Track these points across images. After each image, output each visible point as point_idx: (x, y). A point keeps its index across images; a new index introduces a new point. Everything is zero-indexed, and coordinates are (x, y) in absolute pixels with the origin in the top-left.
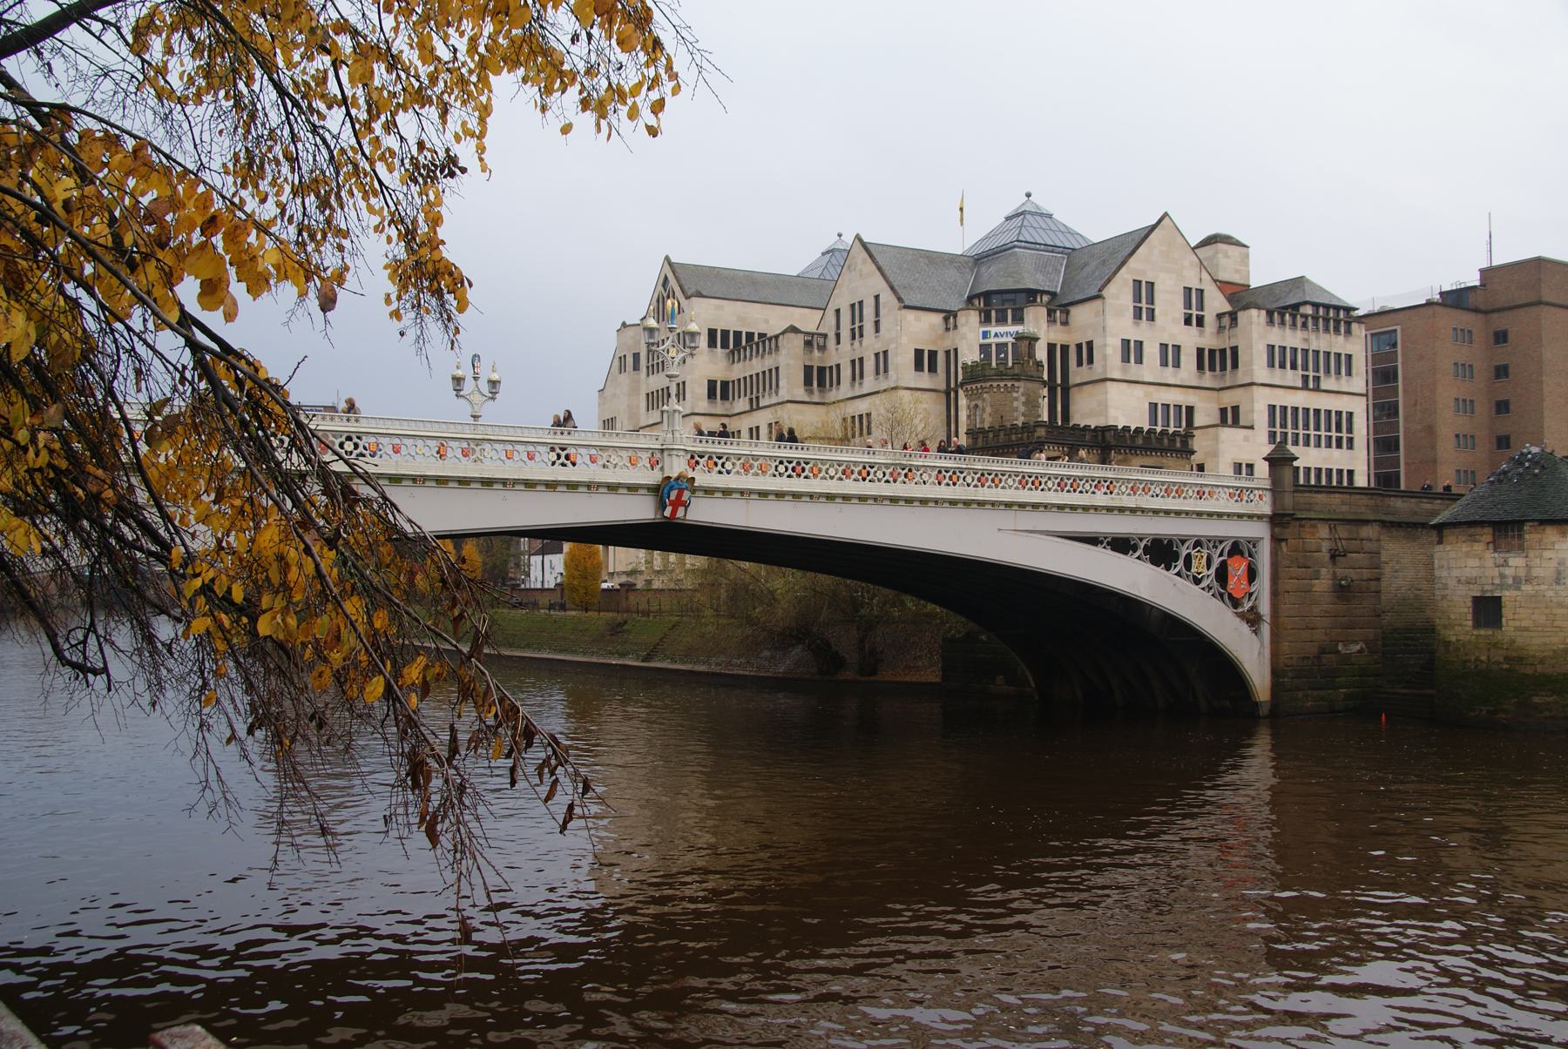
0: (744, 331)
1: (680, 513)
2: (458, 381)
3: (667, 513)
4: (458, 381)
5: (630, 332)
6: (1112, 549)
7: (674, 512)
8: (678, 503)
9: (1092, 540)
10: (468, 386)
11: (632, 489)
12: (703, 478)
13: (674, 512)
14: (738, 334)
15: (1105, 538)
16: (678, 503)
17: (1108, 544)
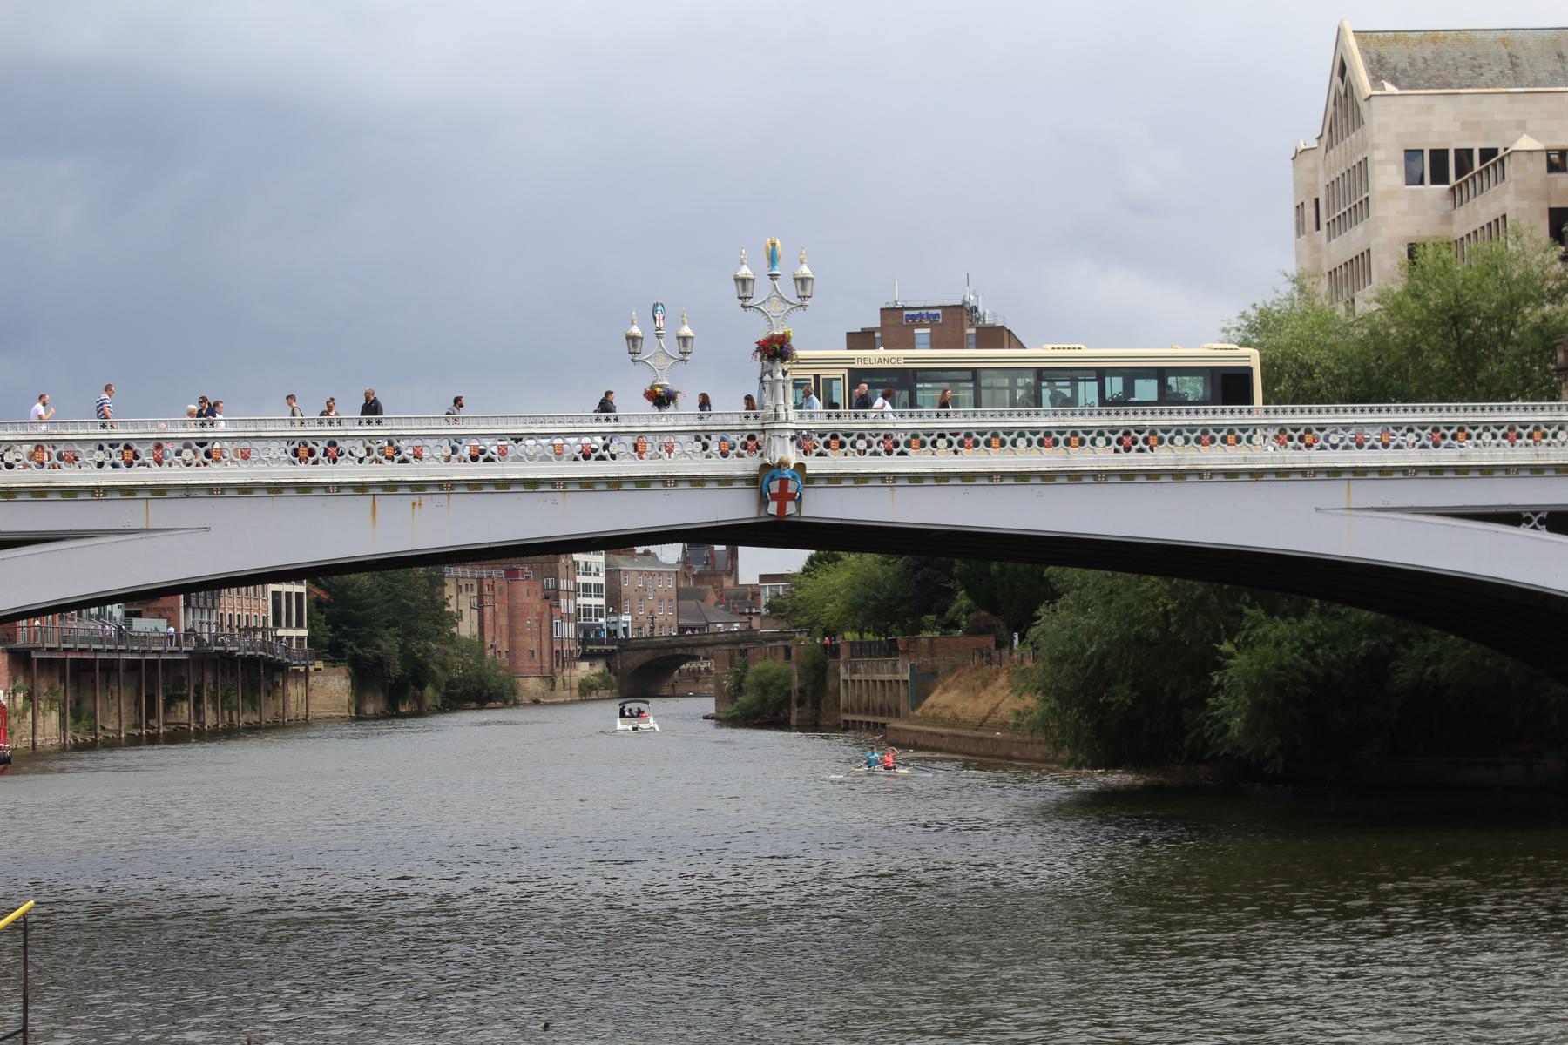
0: (1477, 146)
1: (791, 508)
3: (773, 508)
4: (632, 339)
5: (1308, 162)
6: (1551, 529)
7: (782, 508)
8: (783, 497)
9: (1511, 518)
11: (725, 481)
12: (814, 465)
13: (782, 508)
14: (1464, 156)
15: (1535, 514)
16: (783, 497)
17: (1541, 521)
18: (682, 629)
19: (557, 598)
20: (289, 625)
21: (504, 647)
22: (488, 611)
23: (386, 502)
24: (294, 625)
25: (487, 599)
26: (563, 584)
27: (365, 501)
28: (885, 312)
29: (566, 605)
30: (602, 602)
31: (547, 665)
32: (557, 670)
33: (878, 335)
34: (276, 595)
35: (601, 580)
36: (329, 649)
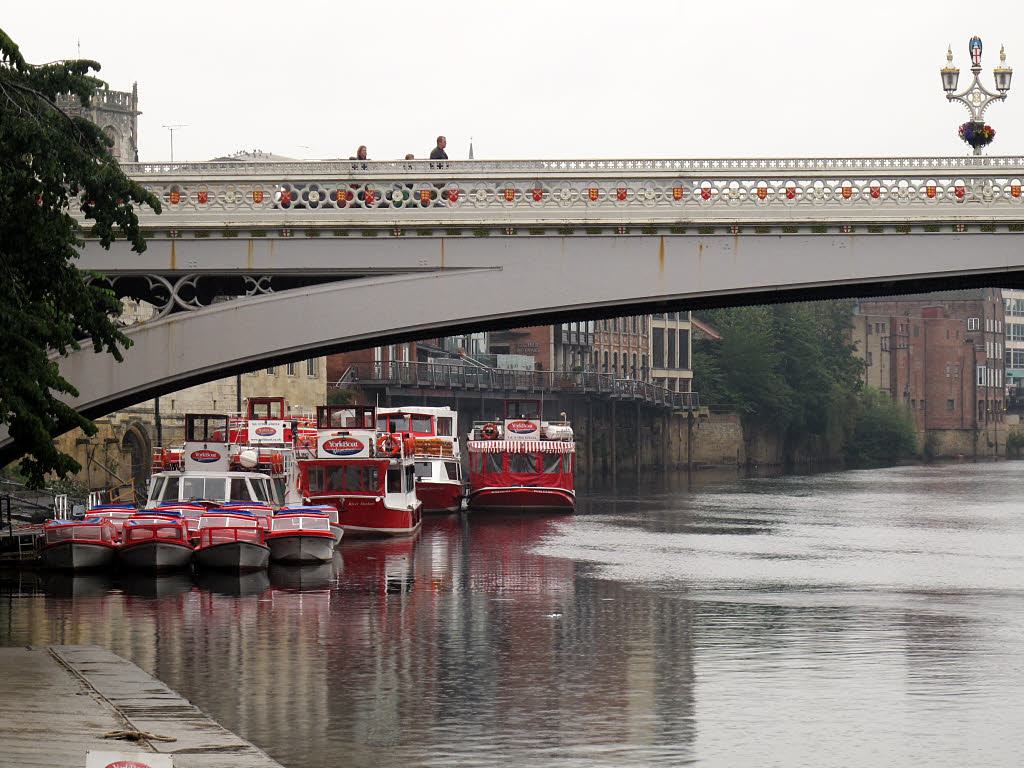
2: (949, 76)
10: (964, 82)
19: (982, 341)
20: (671, 366)
22: (901, 355)
23: (674, 244)
24: (677, 365)
25: (900, 342)
26: (989, 325)
27: (654, 242)
29: (992, 350)
31: (968, 417)
32: (979, 424)
34: (658, 332)
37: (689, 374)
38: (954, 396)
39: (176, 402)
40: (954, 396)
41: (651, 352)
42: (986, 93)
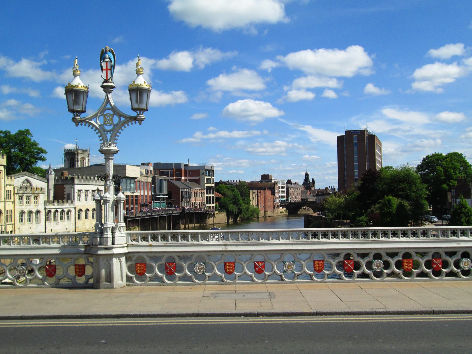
18: (302, 200)
20: (210, 203)
21: (263, 205)
22: (259, 197)
25: (259, 195)
28: (346, 132)
29: (277, 196)
30: (285, 194)
33: (344, 137)
34: (207, 197)
35: (285, 190)
36: (222, 207)
37: (214, 205)
38: (270, 205)
39: (52, 230)
40: (270, 205)
41: (205, 201)
42: (120, 115)
